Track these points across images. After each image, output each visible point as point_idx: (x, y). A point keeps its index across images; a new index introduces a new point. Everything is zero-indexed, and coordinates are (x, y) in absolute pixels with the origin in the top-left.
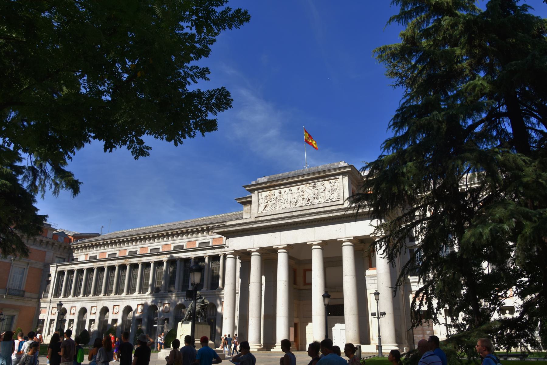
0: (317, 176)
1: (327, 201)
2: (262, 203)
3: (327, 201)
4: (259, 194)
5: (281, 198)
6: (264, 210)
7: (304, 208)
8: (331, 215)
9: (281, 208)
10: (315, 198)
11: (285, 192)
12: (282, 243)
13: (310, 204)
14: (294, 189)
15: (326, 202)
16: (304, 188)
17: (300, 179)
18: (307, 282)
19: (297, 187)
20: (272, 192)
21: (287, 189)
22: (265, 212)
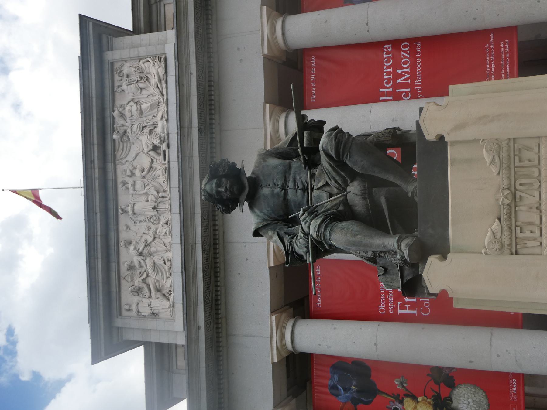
1: (163, 95)
2: (149, 306)
3: (163, 95)
4: (124, 313)
5: (143, 240)
7: (174, 165)
9: (168, 240)
10: (151, 132)
11: (128, 227)
13: (164, 146)
15: (165, 97)
16: (125, 167)
17: (97, 175)
19: (121, 189)
21: (123, 220)
22: (172, 295)
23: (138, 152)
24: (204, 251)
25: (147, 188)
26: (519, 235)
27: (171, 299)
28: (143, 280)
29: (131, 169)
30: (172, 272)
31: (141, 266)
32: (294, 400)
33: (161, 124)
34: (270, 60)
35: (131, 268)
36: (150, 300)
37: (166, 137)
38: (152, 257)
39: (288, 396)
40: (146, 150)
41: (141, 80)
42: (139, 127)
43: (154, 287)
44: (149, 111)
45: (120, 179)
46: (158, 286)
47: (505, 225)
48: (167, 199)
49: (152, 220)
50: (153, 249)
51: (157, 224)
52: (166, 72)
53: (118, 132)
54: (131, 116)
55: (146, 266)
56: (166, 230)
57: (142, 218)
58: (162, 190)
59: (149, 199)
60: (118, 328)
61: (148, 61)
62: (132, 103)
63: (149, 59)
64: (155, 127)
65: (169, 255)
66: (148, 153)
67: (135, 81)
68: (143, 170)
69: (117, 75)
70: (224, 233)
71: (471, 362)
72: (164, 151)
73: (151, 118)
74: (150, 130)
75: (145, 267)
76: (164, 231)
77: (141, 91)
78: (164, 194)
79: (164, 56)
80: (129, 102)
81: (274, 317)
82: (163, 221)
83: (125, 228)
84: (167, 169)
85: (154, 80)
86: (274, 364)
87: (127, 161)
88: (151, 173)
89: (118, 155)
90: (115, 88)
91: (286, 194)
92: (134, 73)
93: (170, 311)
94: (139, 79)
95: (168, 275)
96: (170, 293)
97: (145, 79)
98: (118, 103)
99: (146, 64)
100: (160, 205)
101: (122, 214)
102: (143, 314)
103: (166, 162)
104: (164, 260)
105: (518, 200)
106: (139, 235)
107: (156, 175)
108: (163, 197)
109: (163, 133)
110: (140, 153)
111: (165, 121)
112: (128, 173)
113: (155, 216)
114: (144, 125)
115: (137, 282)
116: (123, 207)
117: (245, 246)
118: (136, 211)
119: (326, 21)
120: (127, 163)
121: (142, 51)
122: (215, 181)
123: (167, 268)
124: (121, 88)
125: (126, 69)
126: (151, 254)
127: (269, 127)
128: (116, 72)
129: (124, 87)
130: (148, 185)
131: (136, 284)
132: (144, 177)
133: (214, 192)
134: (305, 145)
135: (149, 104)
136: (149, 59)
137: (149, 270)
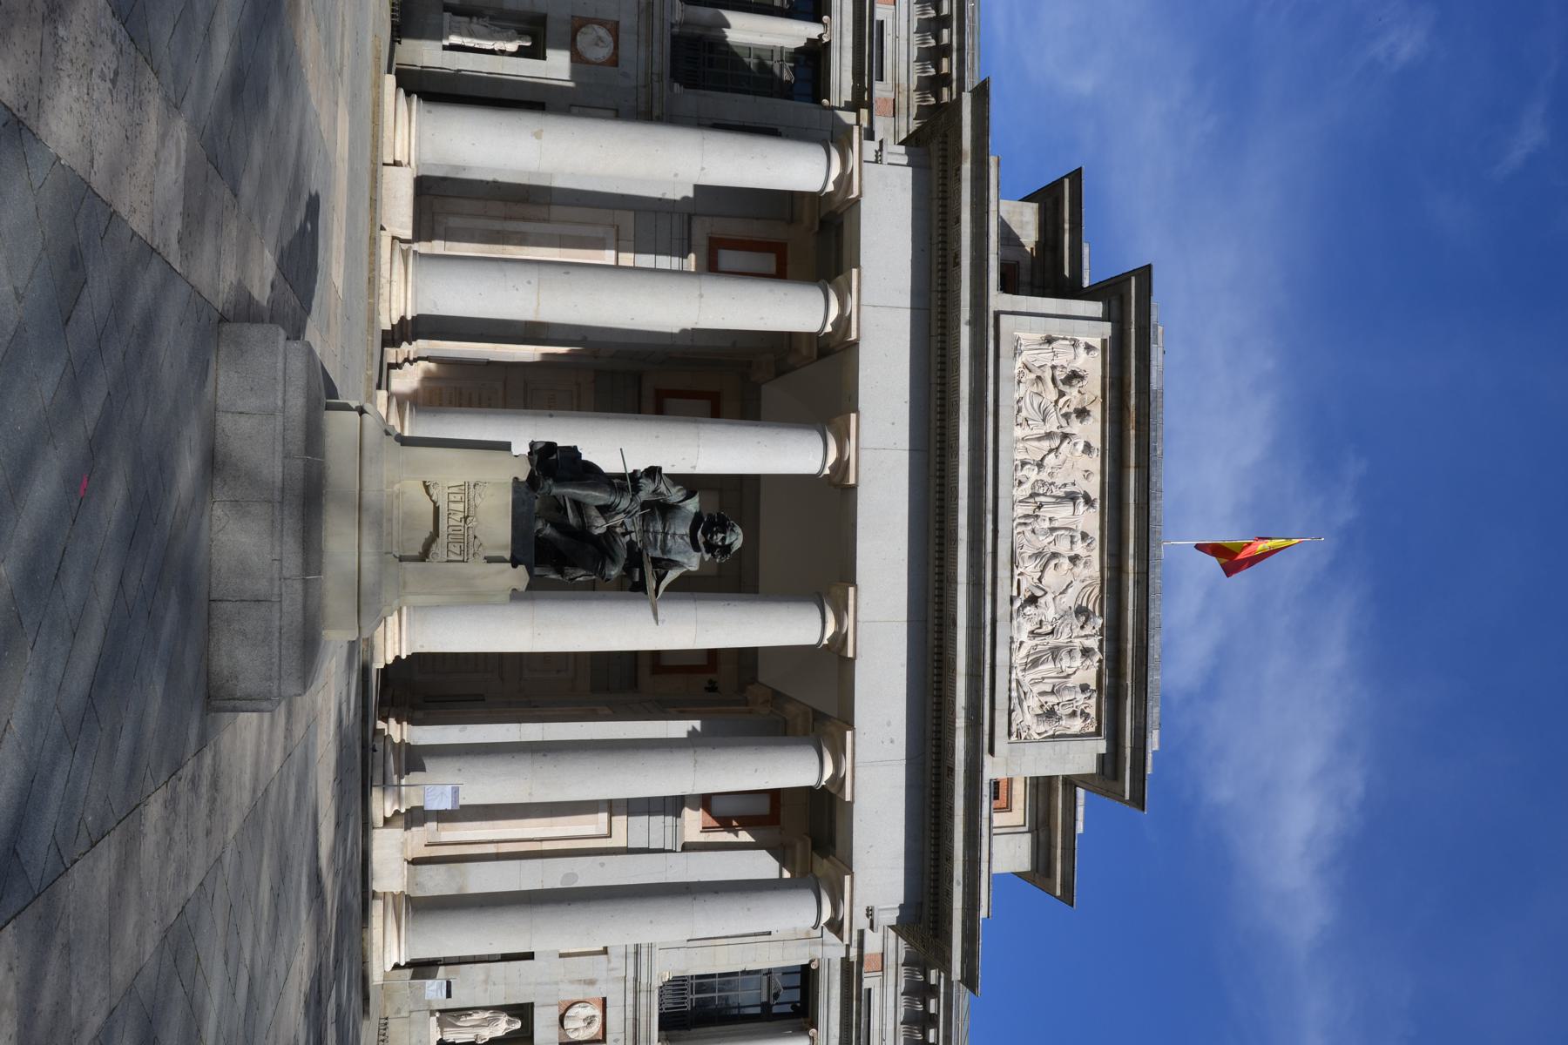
0: (1130, 646)
1: (1018, 682)
2: (1055, 355)
3: (1018, 682)
4: (1096, 342)
5: (1061, 457)
6: (1026, 366)
7: (1003, 573)
8: (960, 723)
11: (1087, 478)
14: (1089, 520)
15: (1014, 676)
16: (1086, 573)
17: (1131, 562)
18: (670, 402)
20: (1096, 411)
21: (1093, 487)
22: (1016, 371)
23: (1063, 596)
24: (957, 438)
25: (1051, 538)
26: (463, 496)
27: (1019, 364)
28: (1064, 395)
29: (1076, 570)
30: (1016, 407)
31: (1066, 416)
32: (834, 207)
33: (1024, 636)
34: (847, 723)
35: (1082, 413)
36: (1054, 363)
37: (1015, 615)
38: (1048, 431)
39: (842, 214)
40: (1049, 597)
41: (1053, 705)
42: (1059, 635)
43: (1046, 383)
44: (1041, 657)
45: (1096, 554)
46: (1040, 385)
47: (472, 502)
48: (1018, 521)
49: (1046, 488)
50: (1046, 445)
51: (1037, 481)
52: (1010, 712)
53: (1094, 628)
54: (1071, 650)
55: (1058, 419)
56: (1022, 469)
57: (1061, 493)
58: (1026, 534)
59: (1047, 522)
60: (1109, 321)
61: (1039, 734)
62: (1070, 671)
63: (1038, 737)
64: (1032, 632)
65: (1019, 432)
66: (1043, 593)
67: (1063, 705)
68: (1056, 564)
69: (1092, 716)
70: (928, 465)
71: (568, 273)
72: (1019, 594)
73: (1039, 647)
74: (1040, 628)
75: (1059, 415)
76: (1026, 471)
77: (1053, 688)
79: (1014, 738)
80: (1075, 672)
81: (854, 336)
82: (1026, 490)
83: (1091, 477)
84: (1015, 567)
85: (1033, 702)
86: (858, 266)
88: (1044, 560)
89: (1097, 590)
90: (1095, 695)
91: (664, 528)
92: (1064, 717)
93: (1021, 344)
94: (1056, 707)
95: (1022, 404)
96: (1021, 375)
97: (1046, 706)
98: (1093, 672)
99: (1042, 729)
100: (1031, 513)
101: (1095, 499)
102: (1067, 342)
103: (1016, 578)
104: (1028, 425)
105: (463, 520)
106: (1068, 465)
107: (1034, 558)
108: (1025, 524)
109: (1019, 623)
110: (1060, 594)
111: (1015, 640)
112: (1081, 564)
113: (1039, 495)
114: (1051, 636)
115: (1073, 393)
116: (1091, 510)
117: (895, 444)
118: (1072, 504)
119: (756, 771)
120: (1083, 578)
121: (1048, 746)
122: (727, 542)
123: (1024, 410)
124: (1085, 696)
125: (1077, 725)
126: (1049, 436)
127: (849, 622)
128: (1092, 721)
129: (1080, 697)
130: (1049, 543)
131: (1074, 391)
133: (728, 533)
134: (638, 569)
135: (1041, 668)
136: (1038, 737)
137: (1053, 410)
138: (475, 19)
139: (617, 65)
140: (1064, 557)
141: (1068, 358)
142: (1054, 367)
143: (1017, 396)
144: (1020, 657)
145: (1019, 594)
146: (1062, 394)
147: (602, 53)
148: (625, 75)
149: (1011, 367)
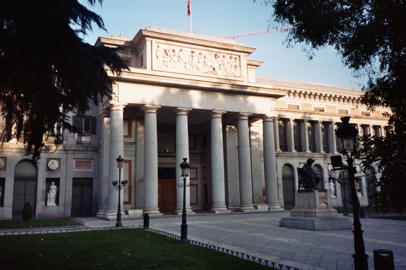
7: (208, 75)
12: (186, 106)
13: (214, 72)
20: (173, 47)
30: (173, 68)
35: (173, 51)
50: (181, 61)
52: (236, 77)
59: (197, 63)
63: (240, 71)
64: (220, 69)
72: (212, 72)
78: (199, 69)
79: (241, 76)
87: (209, 56)
108: (198, 69)
115: (169, 54)
123: (175, 66)
127: (219, 112)
132: (204, 62)
136: (240, 71)
138: (47, 197)
139: (60, 159)
140: (204, 60)
141: (161, 53)
142: (163, 57)
143: (171, 68)
144: (225, 74)
145: (212, 72)
146: (170, 56)
147: (56, 163)
148: (62, 157)
149: (165, 69)
